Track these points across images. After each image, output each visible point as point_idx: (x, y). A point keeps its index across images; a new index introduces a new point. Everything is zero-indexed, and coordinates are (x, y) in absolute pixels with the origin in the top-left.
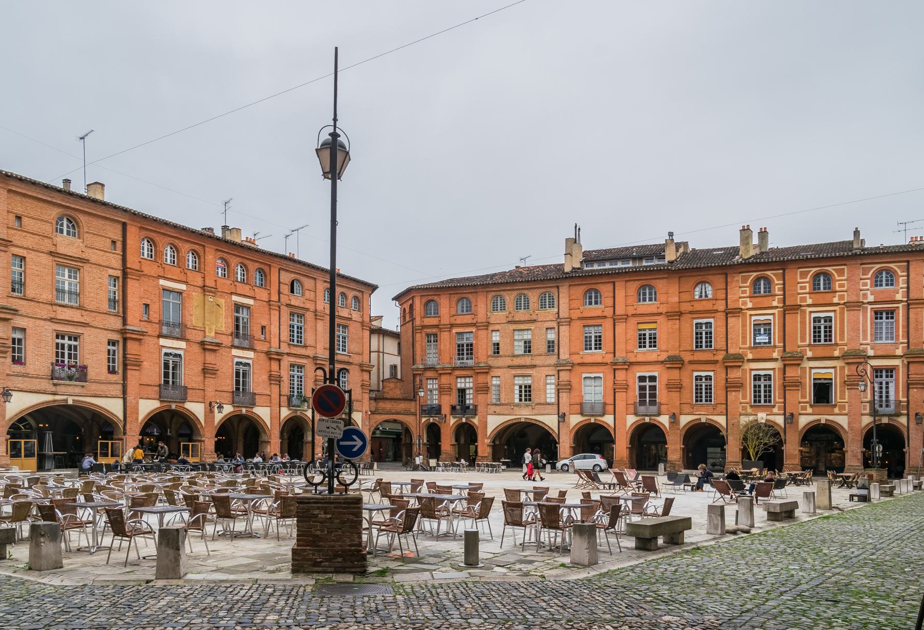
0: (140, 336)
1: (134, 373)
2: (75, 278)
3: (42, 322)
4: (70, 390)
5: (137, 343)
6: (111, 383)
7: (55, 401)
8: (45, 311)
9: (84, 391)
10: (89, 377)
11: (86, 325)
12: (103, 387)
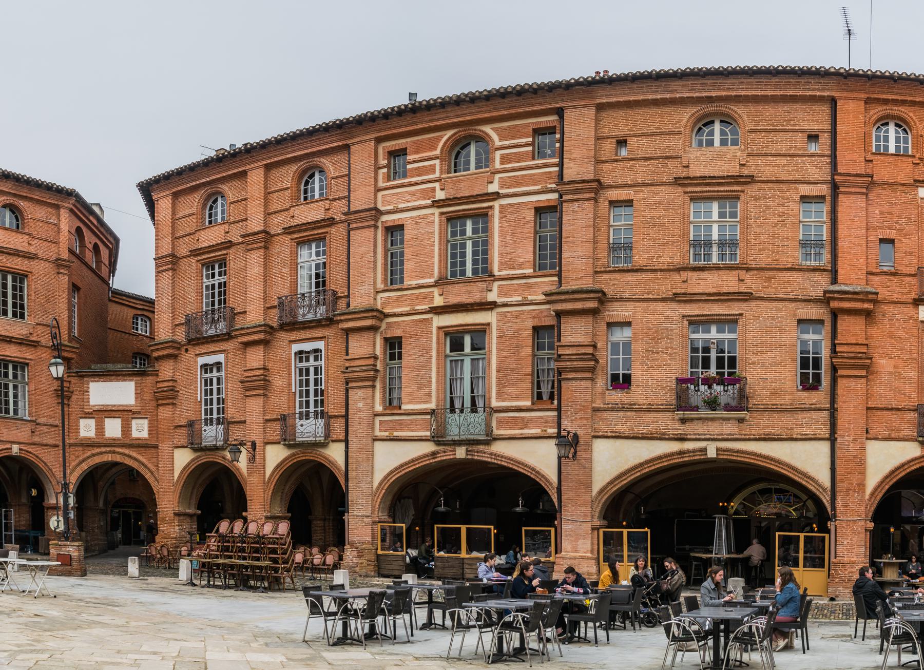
0: (867, 307)
1: (852, 383)
2: (733, 215)
3: (660, 306)
4: (714, 429)
5: (861, 320)
6: (803, 410)
7: (681, 453)
8: (665, 286)
9: (745, 430)
10: (752, 402)
11: (747, 297)
12: (786, 418)
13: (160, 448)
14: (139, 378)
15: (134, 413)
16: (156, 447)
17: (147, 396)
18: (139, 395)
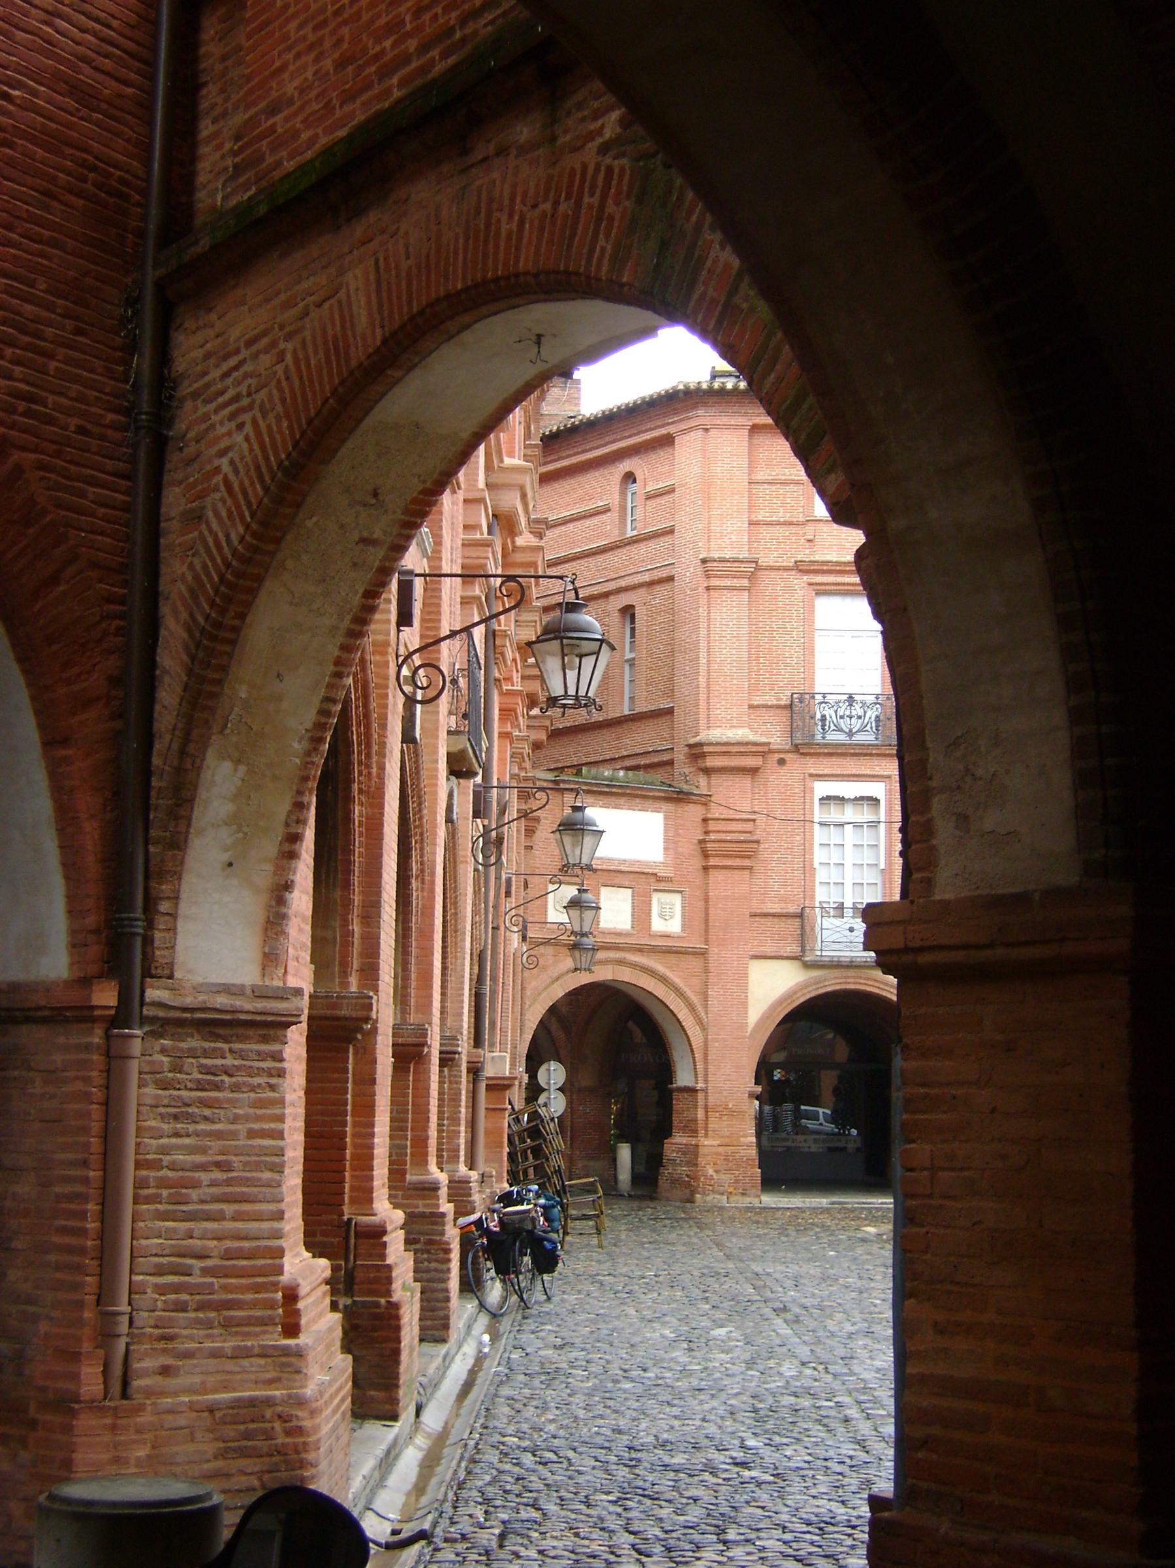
13: (712, 958)
14: (670, 807)
15: (660, 879)
16: (702, 954)
17: (688, 847)
18: (670, 843)
